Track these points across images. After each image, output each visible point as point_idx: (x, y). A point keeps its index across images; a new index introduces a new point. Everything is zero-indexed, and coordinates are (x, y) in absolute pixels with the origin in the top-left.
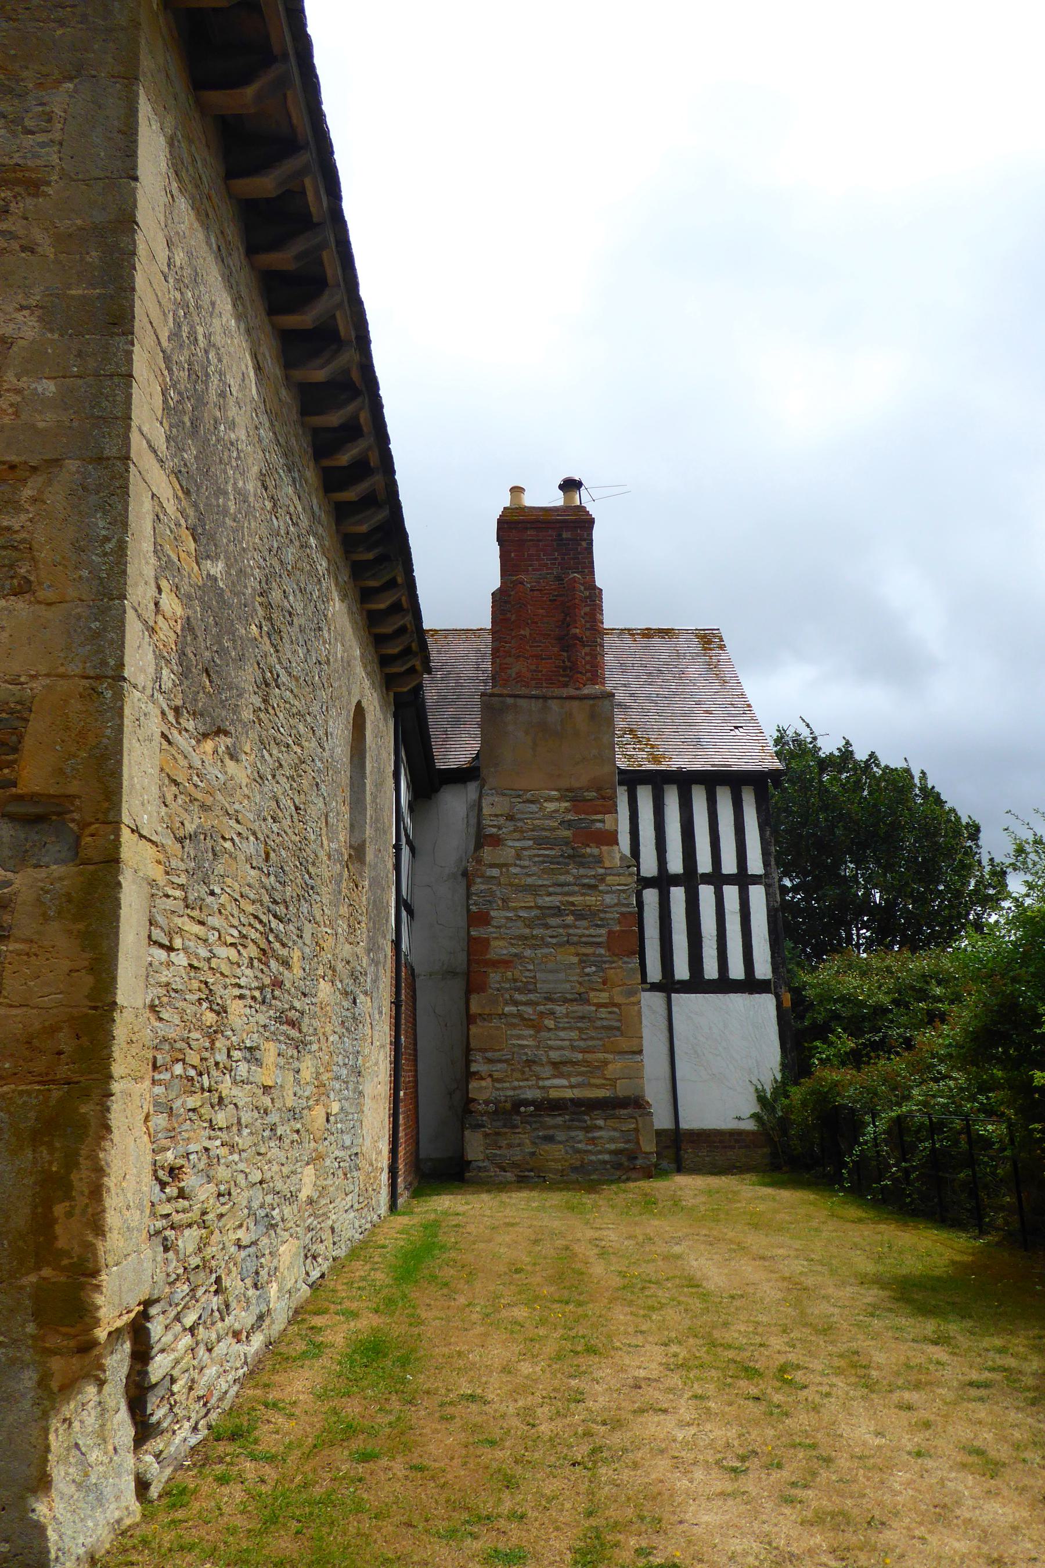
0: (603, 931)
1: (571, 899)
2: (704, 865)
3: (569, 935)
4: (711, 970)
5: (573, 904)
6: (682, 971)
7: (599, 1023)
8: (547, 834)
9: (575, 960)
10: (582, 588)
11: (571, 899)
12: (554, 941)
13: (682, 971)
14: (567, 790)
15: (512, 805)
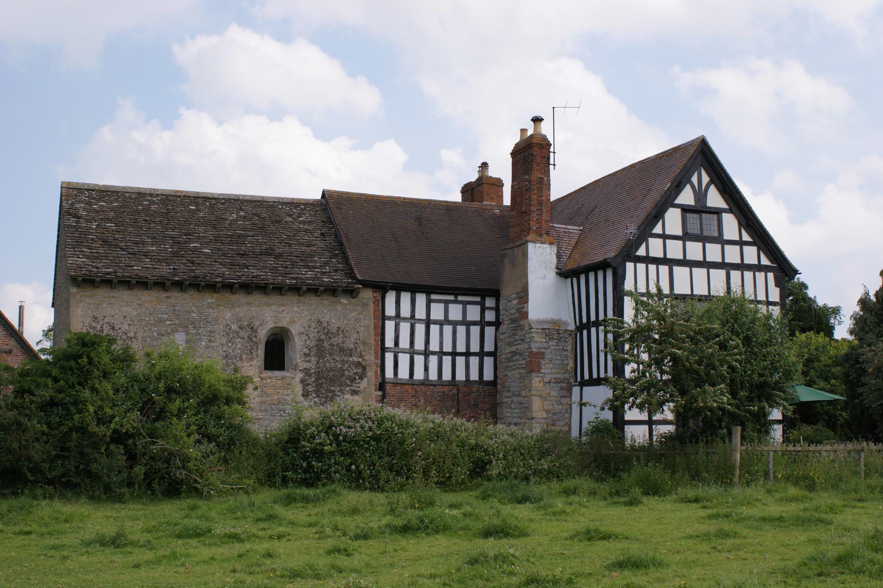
0: (525, 362)
1: (518, 347)
2: (593, 318)
3: (518, 364)
4: (595, 376)
5: (518, 349)
6: (587, 377)
7: (524, 405)
8: (513, 316)
9: (518, 376)
10: (527, 183)
11: (518, 347)
12: (514, 367)
13: (587, 377)
14: (518, 293)
15: (506, 304)
